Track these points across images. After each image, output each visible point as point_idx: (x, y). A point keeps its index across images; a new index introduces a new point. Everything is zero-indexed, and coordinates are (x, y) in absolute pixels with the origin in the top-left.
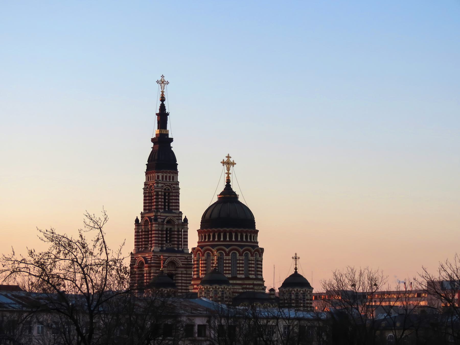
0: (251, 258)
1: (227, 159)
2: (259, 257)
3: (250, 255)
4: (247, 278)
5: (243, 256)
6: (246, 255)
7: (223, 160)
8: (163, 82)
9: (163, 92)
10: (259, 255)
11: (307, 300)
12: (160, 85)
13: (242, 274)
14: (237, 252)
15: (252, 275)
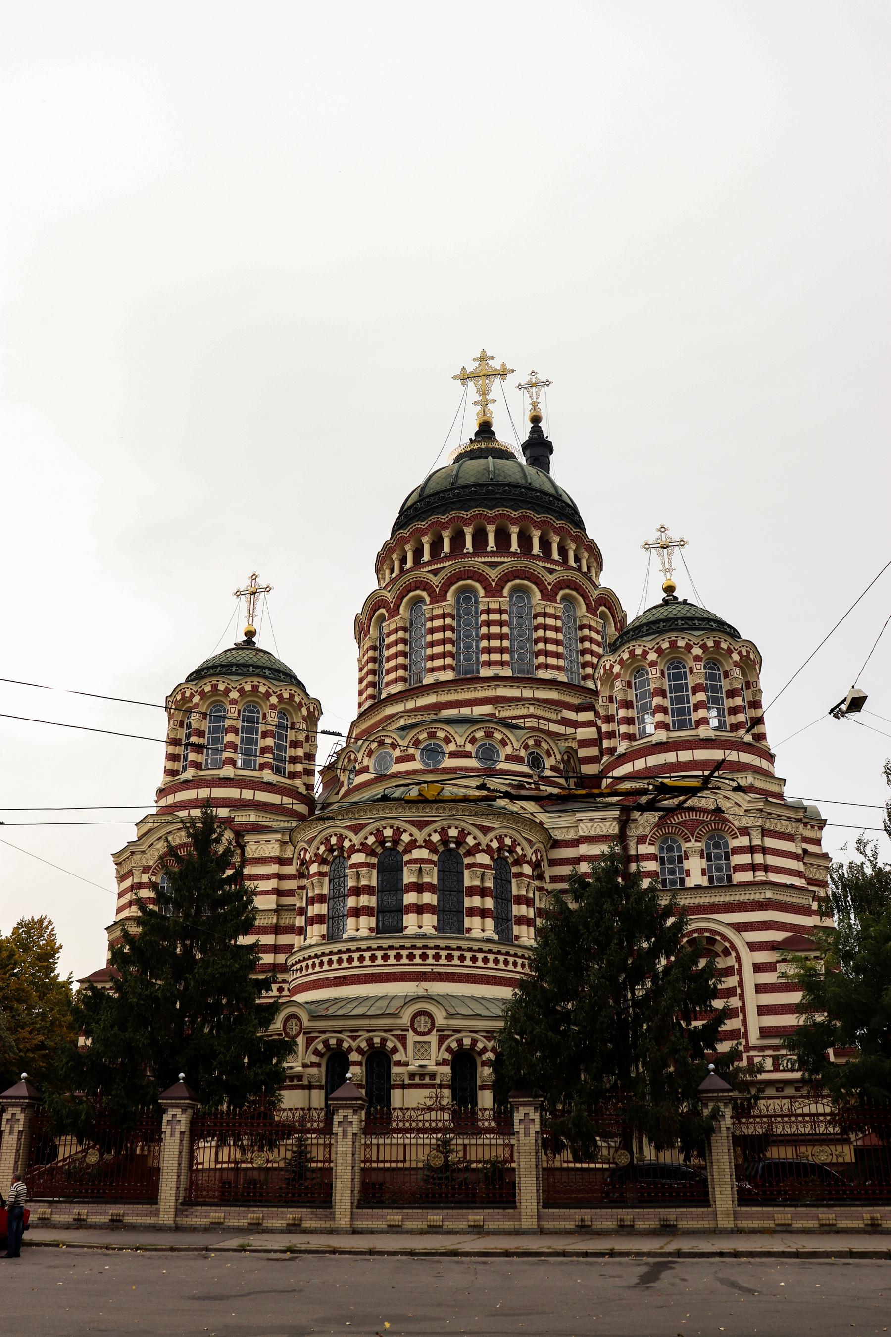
0: (484, 602)
1: (477, 363)
2: (542, 599)
3: (482, 592)
4: (468, 679)
5: (445, 600)
6: (466, 594)
7: (464, 369)
8: (534, 385)
9: (535, 405)
10: (538, 595)
11: (695, 691)
12: (525, 391)
13: (444, 668)
14: (424, 594)
15: (492, 668)
